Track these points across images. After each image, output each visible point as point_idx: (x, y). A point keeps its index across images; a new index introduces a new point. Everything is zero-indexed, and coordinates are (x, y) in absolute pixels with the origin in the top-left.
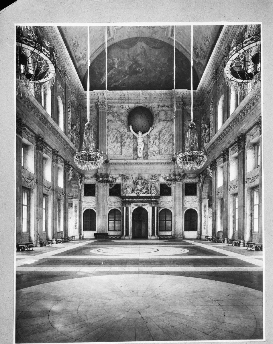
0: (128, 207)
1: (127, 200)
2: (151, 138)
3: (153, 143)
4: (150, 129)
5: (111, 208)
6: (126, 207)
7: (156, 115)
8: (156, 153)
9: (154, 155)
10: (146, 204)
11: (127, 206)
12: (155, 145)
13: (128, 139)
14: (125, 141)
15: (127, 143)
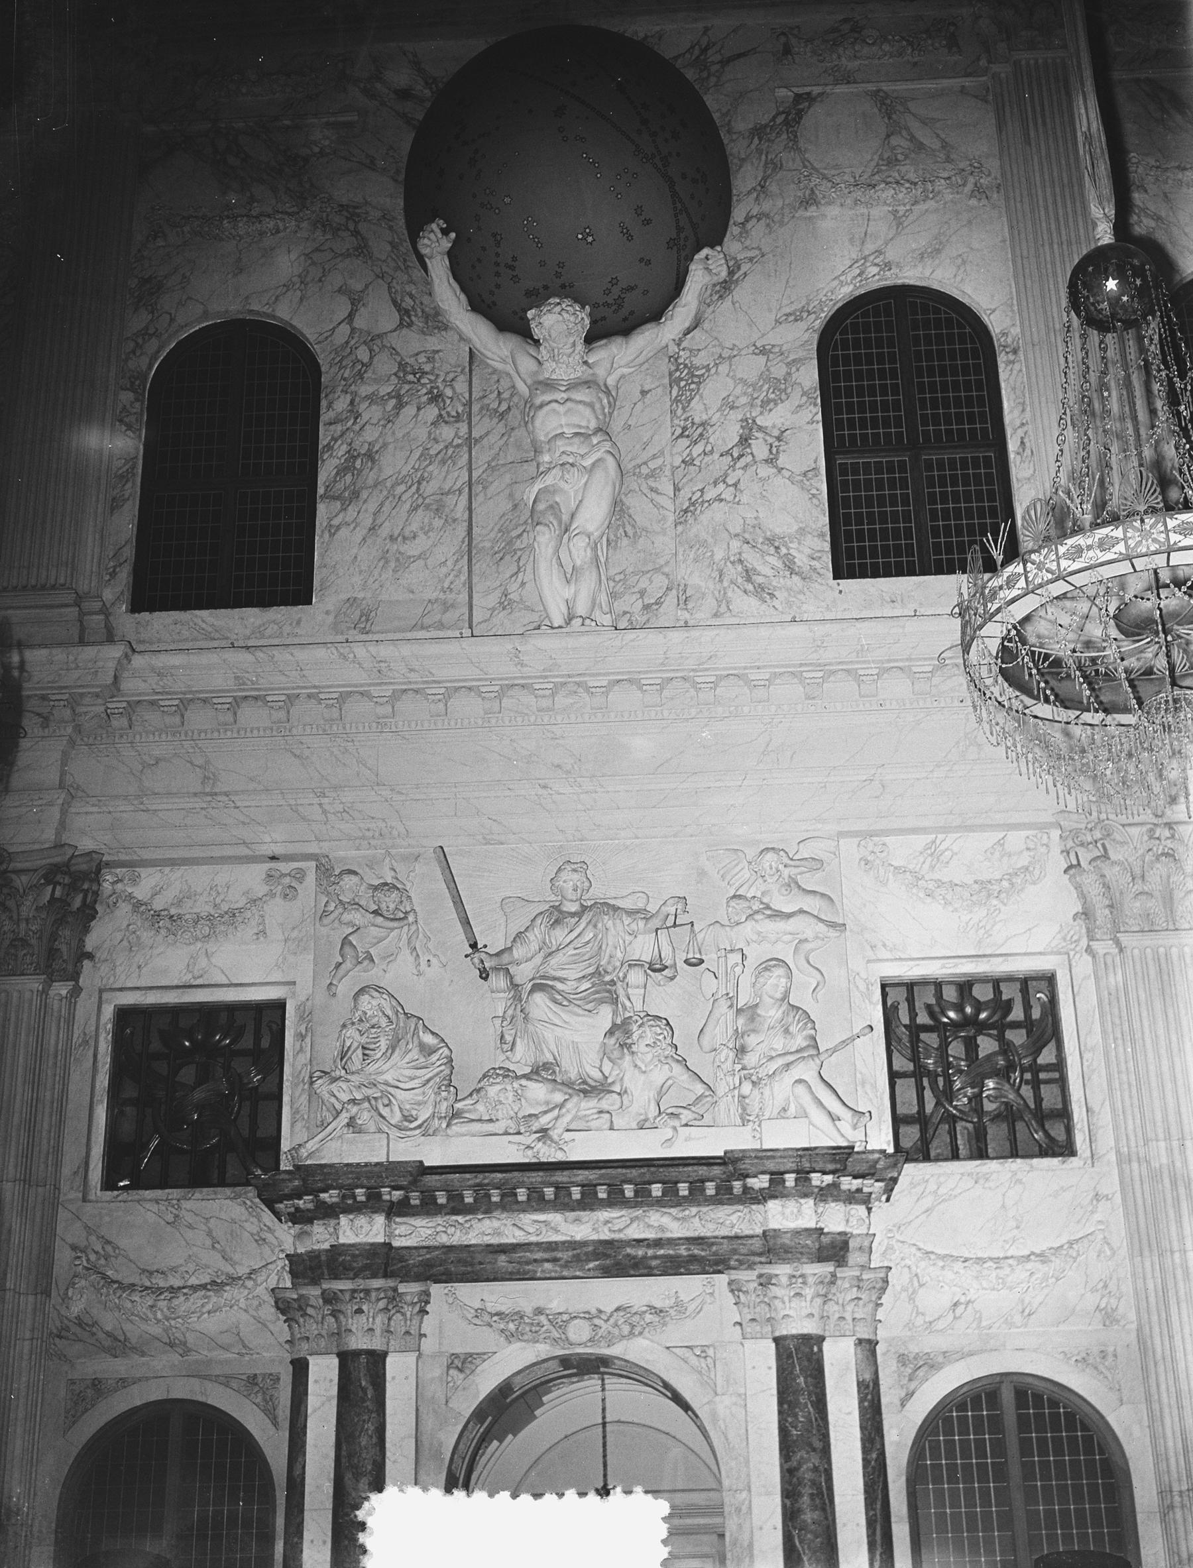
0: (377, 1359)
1: (362, 1230)
2: (714, 391)
3: (744, 441)
4: (697, 279)
5: (123, 1383)
6: (346, 1359)
7: (759, 131)
8: (790, 567)
9: (763, 592)
10: (679, 1306)
11: (358, 1342)
12: (765, 471)
13: (410, 410)
14: (370, 434)
15: (393, 464)
